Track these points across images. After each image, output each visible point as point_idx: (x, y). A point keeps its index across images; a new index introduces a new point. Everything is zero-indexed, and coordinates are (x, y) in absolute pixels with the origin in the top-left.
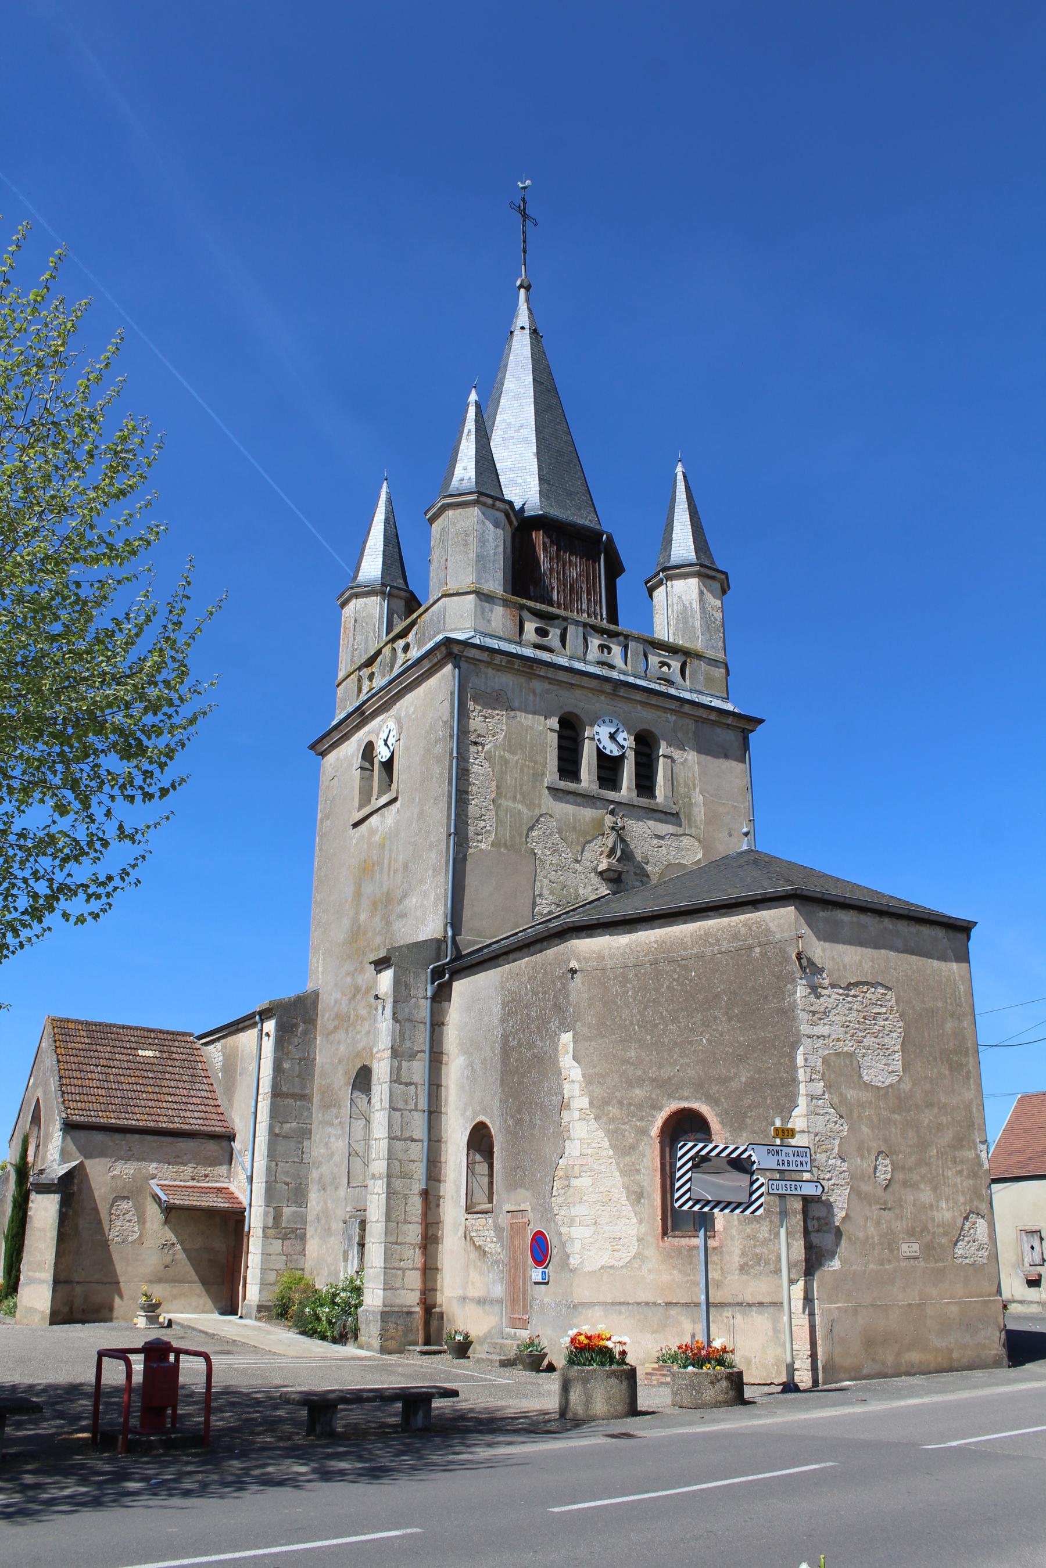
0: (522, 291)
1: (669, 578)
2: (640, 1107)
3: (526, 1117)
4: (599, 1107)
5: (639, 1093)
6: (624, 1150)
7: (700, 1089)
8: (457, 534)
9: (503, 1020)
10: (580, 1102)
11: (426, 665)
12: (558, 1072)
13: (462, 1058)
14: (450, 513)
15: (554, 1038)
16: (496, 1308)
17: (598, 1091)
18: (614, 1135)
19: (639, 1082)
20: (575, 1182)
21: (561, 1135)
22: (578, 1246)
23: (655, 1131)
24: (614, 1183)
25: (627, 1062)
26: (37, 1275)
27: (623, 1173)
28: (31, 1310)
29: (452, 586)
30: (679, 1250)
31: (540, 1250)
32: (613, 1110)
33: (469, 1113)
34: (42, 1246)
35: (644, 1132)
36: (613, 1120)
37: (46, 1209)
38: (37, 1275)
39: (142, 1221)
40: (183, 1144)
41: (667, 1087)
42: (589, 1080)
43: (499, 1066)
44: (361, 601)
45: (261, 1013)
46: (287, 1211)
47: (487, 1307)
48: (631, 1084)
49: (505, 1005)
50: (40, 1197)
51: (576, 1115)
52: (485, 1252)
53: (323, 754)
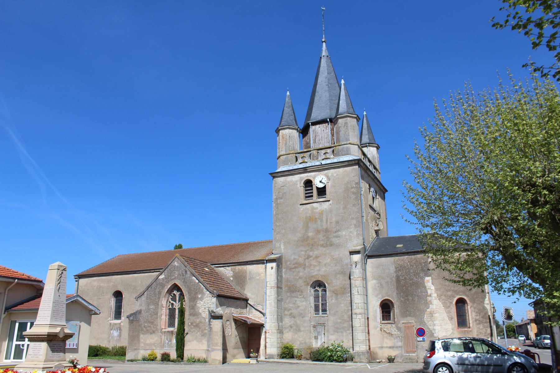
0: (324, 44)
1: (369, 146)
2: (450, 297)
3: (410, 298)
4: (440, 297)
5: (449, 293)
6: (447, 307)
7: (464, 293)
8: (351, 126)
9: (396, 272)
10: (435, 295)
11: (346, 163)
12: (425, 287)
13: (375, 281)
14: (349, 118)
15: (423, 278)
16: (400, 349)
17: (439, 293)
18: (444, 304)
19: (449, 290)
20: (435, 315)
21: (427, 304)
22: (437, 331)
23: (454, 302)
24: (445, 315)
25: (445, 285)
26: (216, 348)
27: (447, 313)
28: (215, 360)
29: (351, 141)
30: (462, 331)
31: (421, 332)
32: (443, 297)
33: (380, 296)
34: (217, 338)
35: (451, 303)
36: (443, 300)
37: (217, 325)
38: (216, 348)
39: (231, 329)
40: (239, 302)
41: (457, 292)
42: (436, 290)
43: (395, 284)
44: (291, 130)
45: (266, 260)
46: (280, 324)
47: (395, 349)
48: (447, 291)
49: (396, 268)
50: (214, 320)
51: (434, 298)
52: (392, 334)
53: (274, 177)
